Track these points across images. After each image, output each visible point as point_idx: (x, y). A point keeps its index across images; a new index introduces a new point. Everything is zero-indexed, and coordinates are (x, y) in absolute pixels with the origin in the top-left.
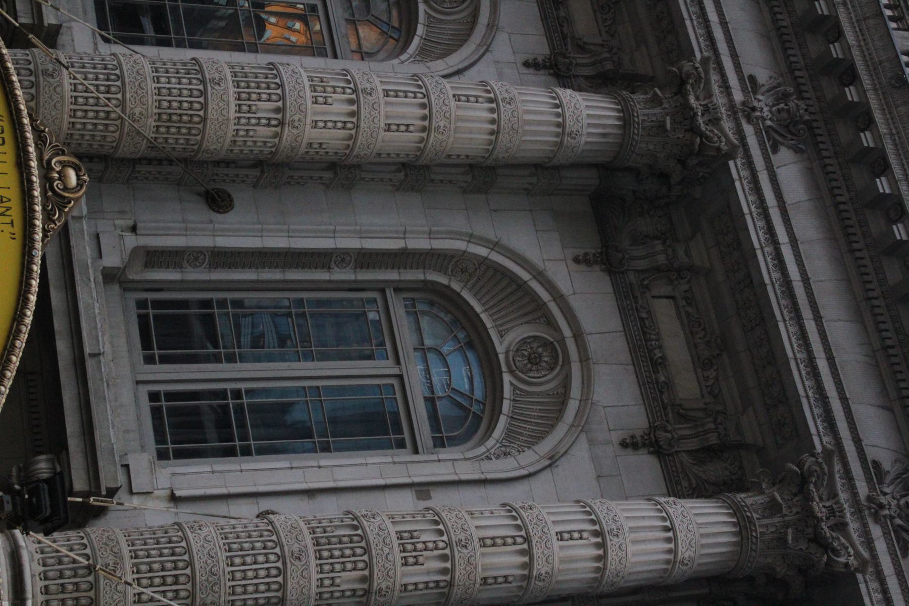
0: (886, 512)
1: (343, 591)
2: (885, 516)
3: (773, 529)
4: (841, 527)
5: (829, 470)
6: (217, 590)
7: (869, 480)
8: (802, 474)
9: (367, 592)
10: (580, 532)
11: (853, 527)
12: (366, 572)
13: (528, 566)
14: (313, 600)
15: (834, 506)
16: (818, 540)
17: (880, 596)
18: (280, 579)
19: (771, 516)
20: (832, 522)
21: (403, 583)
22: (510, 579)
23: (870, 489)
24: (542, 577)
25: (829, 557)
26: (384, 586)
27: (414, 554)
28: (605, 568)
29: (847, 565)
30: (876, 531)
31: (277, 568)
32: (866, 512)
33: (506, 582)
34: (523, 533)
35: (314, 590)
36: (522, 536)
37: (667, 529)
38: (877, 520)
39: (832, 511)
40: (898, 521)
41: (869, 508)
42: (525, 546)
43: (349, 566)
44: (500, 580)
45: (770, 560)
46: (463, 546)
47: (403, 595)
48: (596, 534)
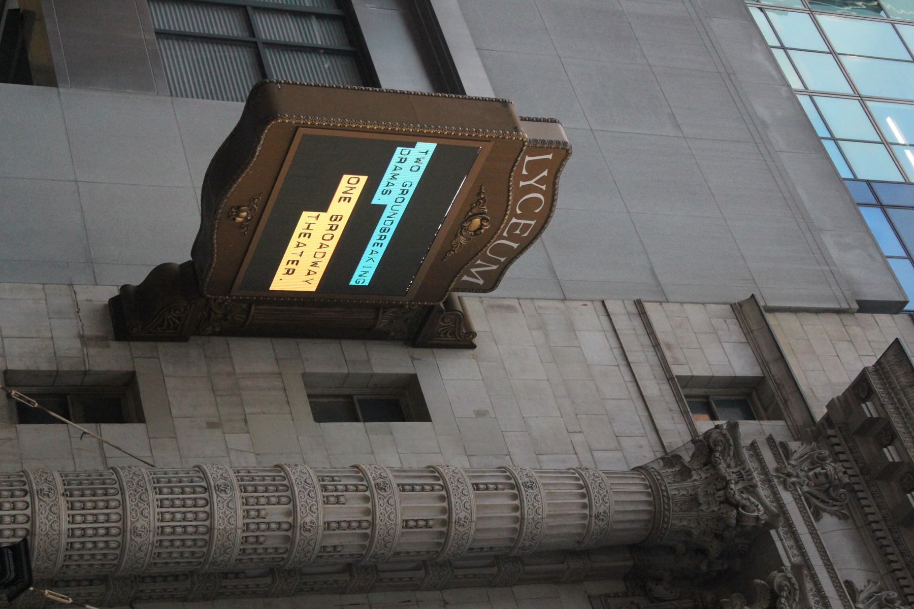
0: (794, 479)
1: (268, 523)
2: (793, 484)
3: (685, 493)
4: (751, 489)
5: (734, 441)
6: (147, 515)
7: (776, 455)
8: (709, 445)
9: (292, 527)
10: (496, 484)
11: (763, 492)
12: (290, 506)
13: (448, 511)
14: (240, 531)
15: (743, 472)
16: (728, 501)
17: (796, 552)
18: (207, 509)
19: (684, 480)
20: (740, 486)
21: (326, 520)
22: (431, 523)
23: (778, 463)
24: (462, 523)
25: (738, 513)
26: (308, 520)
27: (335, 494)
28: (523, 518)
29: (757, 518)
30: (787, 497)
31: (205, 499)
32: (776, 481)
33: (427, 526)
34: (441, 482)
35: (240, 522)
36: (440, 485)
37: (581, 487)
38: (786, 488)
39: (741, 477)
40: (806, 488)
41: (779, 478)
42: (444, 493)
43: (273, 500)
44: (421, 523)
45: (685, 523)
46: (381, 489)
47: (326, 532)
48: (512, 487)
